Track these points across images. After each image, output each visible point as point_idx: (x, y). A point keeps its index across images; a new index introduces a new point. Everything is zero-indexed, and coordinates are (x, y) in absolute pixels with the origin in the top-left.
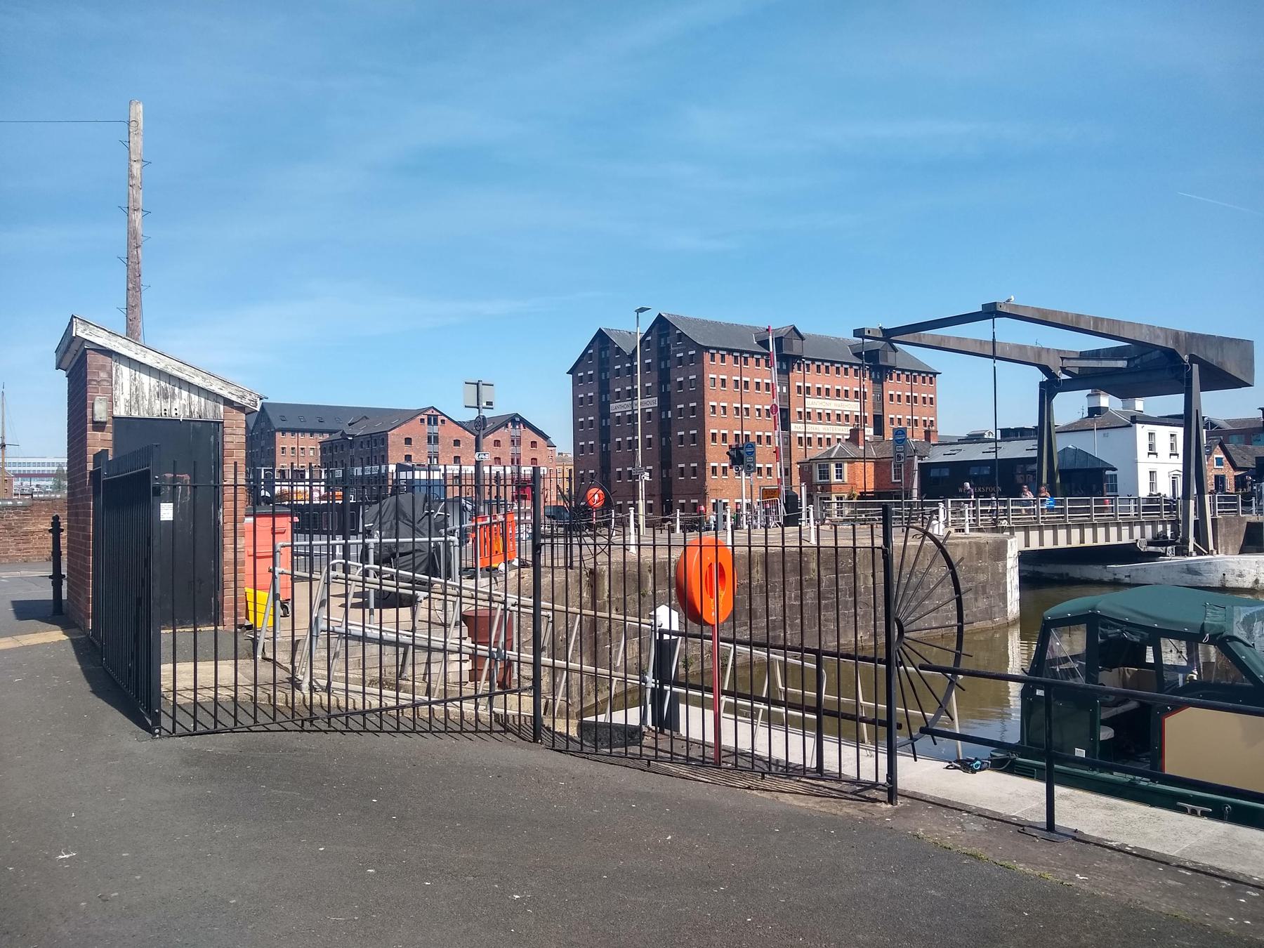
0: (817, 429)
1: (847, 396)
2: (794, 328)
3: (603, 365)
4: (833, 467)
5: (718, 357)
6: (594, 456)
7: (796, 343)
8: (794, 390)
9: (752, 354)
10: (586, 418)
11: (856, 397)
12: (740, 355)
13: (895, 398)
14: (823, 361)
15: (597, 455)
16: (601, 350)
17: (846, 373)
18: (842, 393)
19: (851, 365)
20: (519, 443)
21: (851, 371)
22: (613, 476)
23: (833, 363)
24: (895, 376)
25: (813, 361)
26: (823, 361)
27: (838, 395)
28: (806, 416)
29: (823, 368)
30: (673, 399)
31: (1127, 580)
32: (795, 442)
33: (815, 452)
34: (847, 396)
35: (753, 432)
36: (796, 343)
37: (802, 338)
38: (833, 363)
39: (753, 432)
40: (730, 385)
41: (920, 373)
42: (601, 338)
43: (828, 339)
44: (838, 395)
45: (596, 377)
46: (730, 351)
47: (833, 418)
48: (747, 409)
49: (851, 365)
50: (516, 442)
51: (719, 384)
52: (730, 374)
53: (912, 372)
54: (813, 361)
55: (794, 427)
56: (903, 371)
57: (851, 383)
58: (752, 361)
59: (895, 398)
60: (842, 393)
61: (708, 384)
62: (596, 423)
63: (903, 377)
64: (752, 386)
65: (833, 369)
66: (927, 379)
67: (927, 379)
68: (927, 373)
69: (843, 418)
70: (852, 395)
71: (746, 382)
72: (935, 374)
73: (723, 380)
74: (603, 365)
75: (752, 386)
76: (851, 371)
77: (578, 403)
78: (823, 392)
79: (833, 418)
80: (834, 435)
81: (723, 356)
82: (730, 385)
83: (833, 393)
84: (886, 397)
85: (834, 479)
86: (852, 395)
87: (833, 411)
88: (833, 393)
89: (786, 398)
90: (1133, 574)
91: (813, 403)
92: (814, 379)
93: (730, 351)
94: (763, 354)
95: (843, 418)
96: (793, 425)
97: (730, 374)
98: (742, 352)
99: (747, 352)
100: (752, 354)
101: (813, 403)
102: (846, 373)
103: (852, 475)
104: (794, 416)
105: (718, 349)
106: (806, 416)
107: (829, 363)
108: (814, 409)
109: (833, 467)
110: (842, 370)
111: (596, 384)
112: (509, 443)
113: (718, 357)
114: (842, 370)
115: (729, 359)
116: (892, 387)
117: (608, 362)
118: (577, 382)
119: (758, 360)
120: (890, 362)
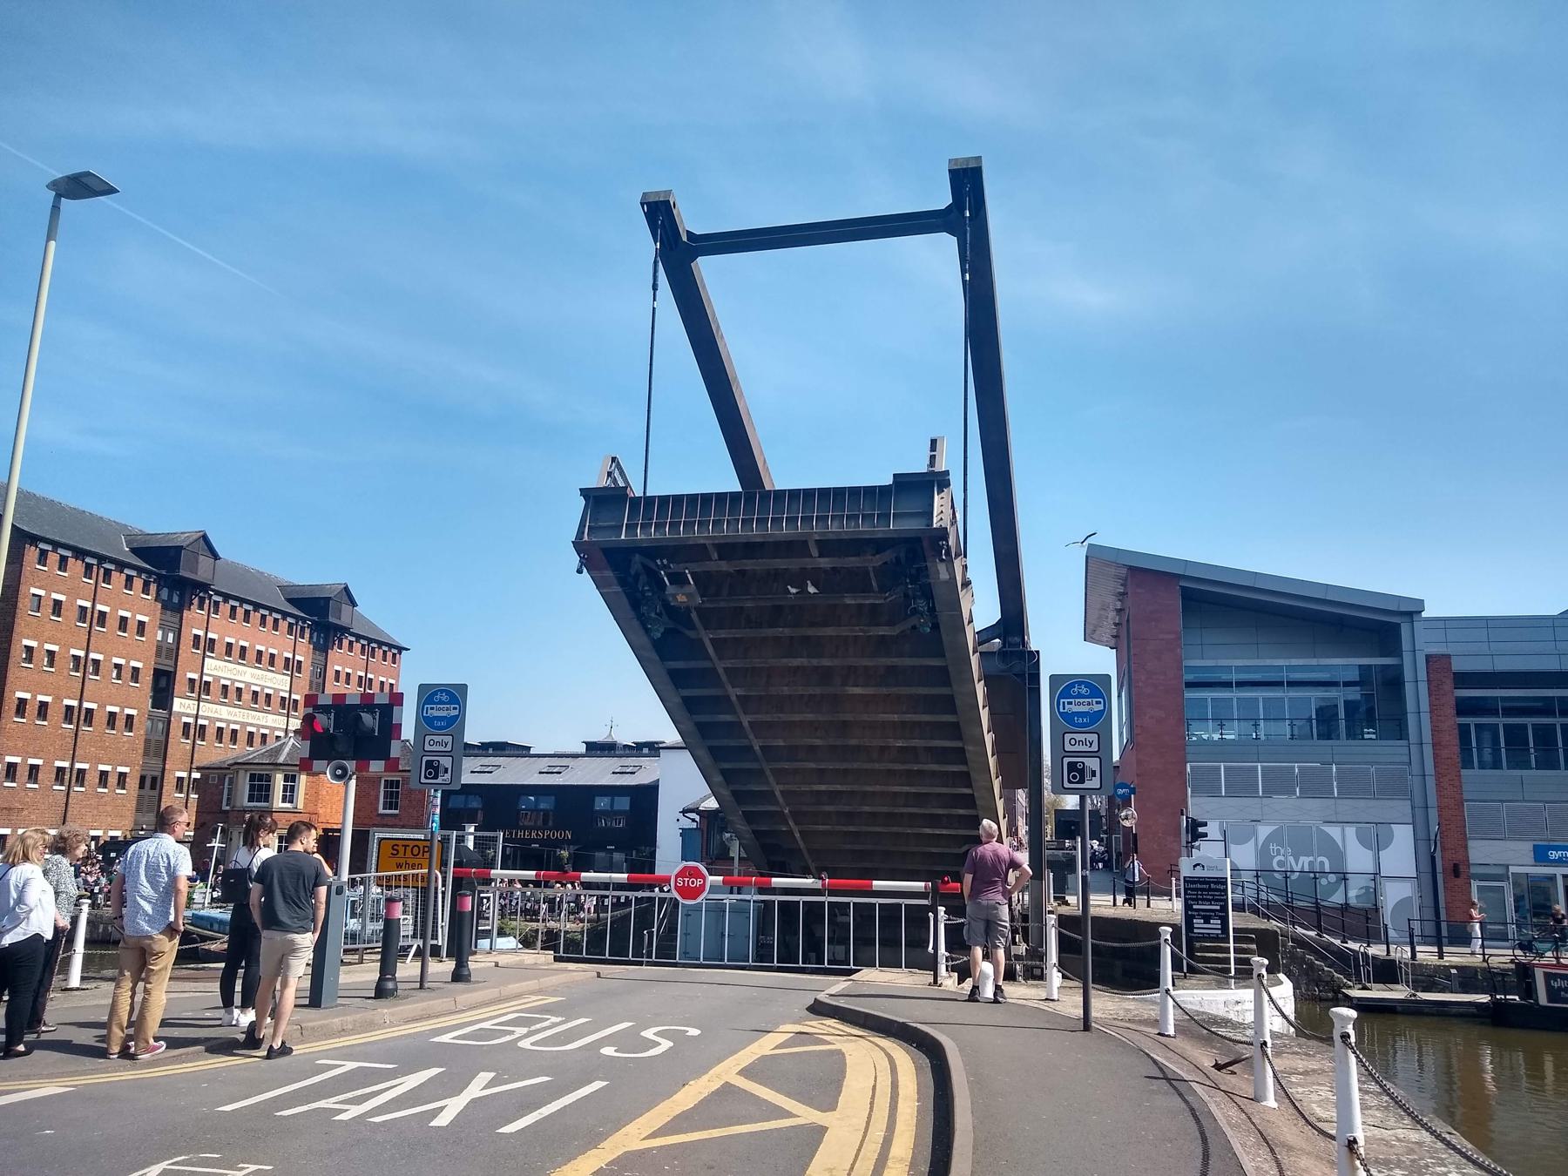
0: (216, 713)
1: (272, 663)
2: (205, 537)
4: (279, 780)
5: (53, 558)
7: (205, 562)
8: (186, 641)
9: (121, 566)
11: (286, 667)
12: (98, 563)
13: (343, 677)
14: (242, 601)
17: (276, 627)
18: (266, 659)
19: (285, 615)
21: (283, 625)
23: (257, 606)
24: (345, 643)
25: (227, 597)
26: (242, 601)
27: (259, 660)
28: (202, 689)
29: (240, 612)
32: (176, 730)
33: (213, 753)
34: (272, 663)
35: (102, 706)
36: (205, 562)
37: (216, 556)
38: (257, 606)
39: (102, 706)
40: (70, 614)
41: (381, 644)
43: (246, 570)
44: (259, 660)
46: (80, 553)
47: (247, 696)
48: (96, 662)
49: (285, 615)
51: (47, 608)
52: (73, 594)
53: (370, 640)
54: (227, 597)
55: (178, 705)
56: (359, 637)
57: (279, 643)
58: (118, 578)
59: (343, 677)
60: (266, 659)
61: (24, 604)
63: (357, 646)
64: (113, 623)
65: (255, 617)
66: (389, 655)
67: (389, 655)
68: (391, 646)
69: (261, 699)
70: (280, 663)
71: (102, 614)
72: (401, 649)
73: (57, 603)
75: (113, 623)
76: (283, 625)
78: (236, 652)
79: (247, 696)
80: (244, 725)
81: (64, 560)
82: (70, 614)
83: (251, 655)
84: (330, 675)
85: (278, 803)
86: (280, 663)
87: (248, 685)
88: (251, 655)
89: (174, 652)
91: (217, 669)
92: (224, 629)
93: (80, 553)
94: (140, 570)
95: (261, 699)
96: (177, 701)
97: (73, 594)
98: (102, 559)
99: (112, 561)
100: (121, 566)
101: (217, 669)
102: (276, 627)
103: (314, 796)
104: (180, 686)
105: (56, 545)
106: (202, 689)
107: (249, 605)
108: (217, 679)
109: (279, 780)
110: (270, 620)
113: (53, 558)
114: (270, 620)
115: (76, 566)
116: (344, 661)
119: (129, 579)
120: (344, 621)
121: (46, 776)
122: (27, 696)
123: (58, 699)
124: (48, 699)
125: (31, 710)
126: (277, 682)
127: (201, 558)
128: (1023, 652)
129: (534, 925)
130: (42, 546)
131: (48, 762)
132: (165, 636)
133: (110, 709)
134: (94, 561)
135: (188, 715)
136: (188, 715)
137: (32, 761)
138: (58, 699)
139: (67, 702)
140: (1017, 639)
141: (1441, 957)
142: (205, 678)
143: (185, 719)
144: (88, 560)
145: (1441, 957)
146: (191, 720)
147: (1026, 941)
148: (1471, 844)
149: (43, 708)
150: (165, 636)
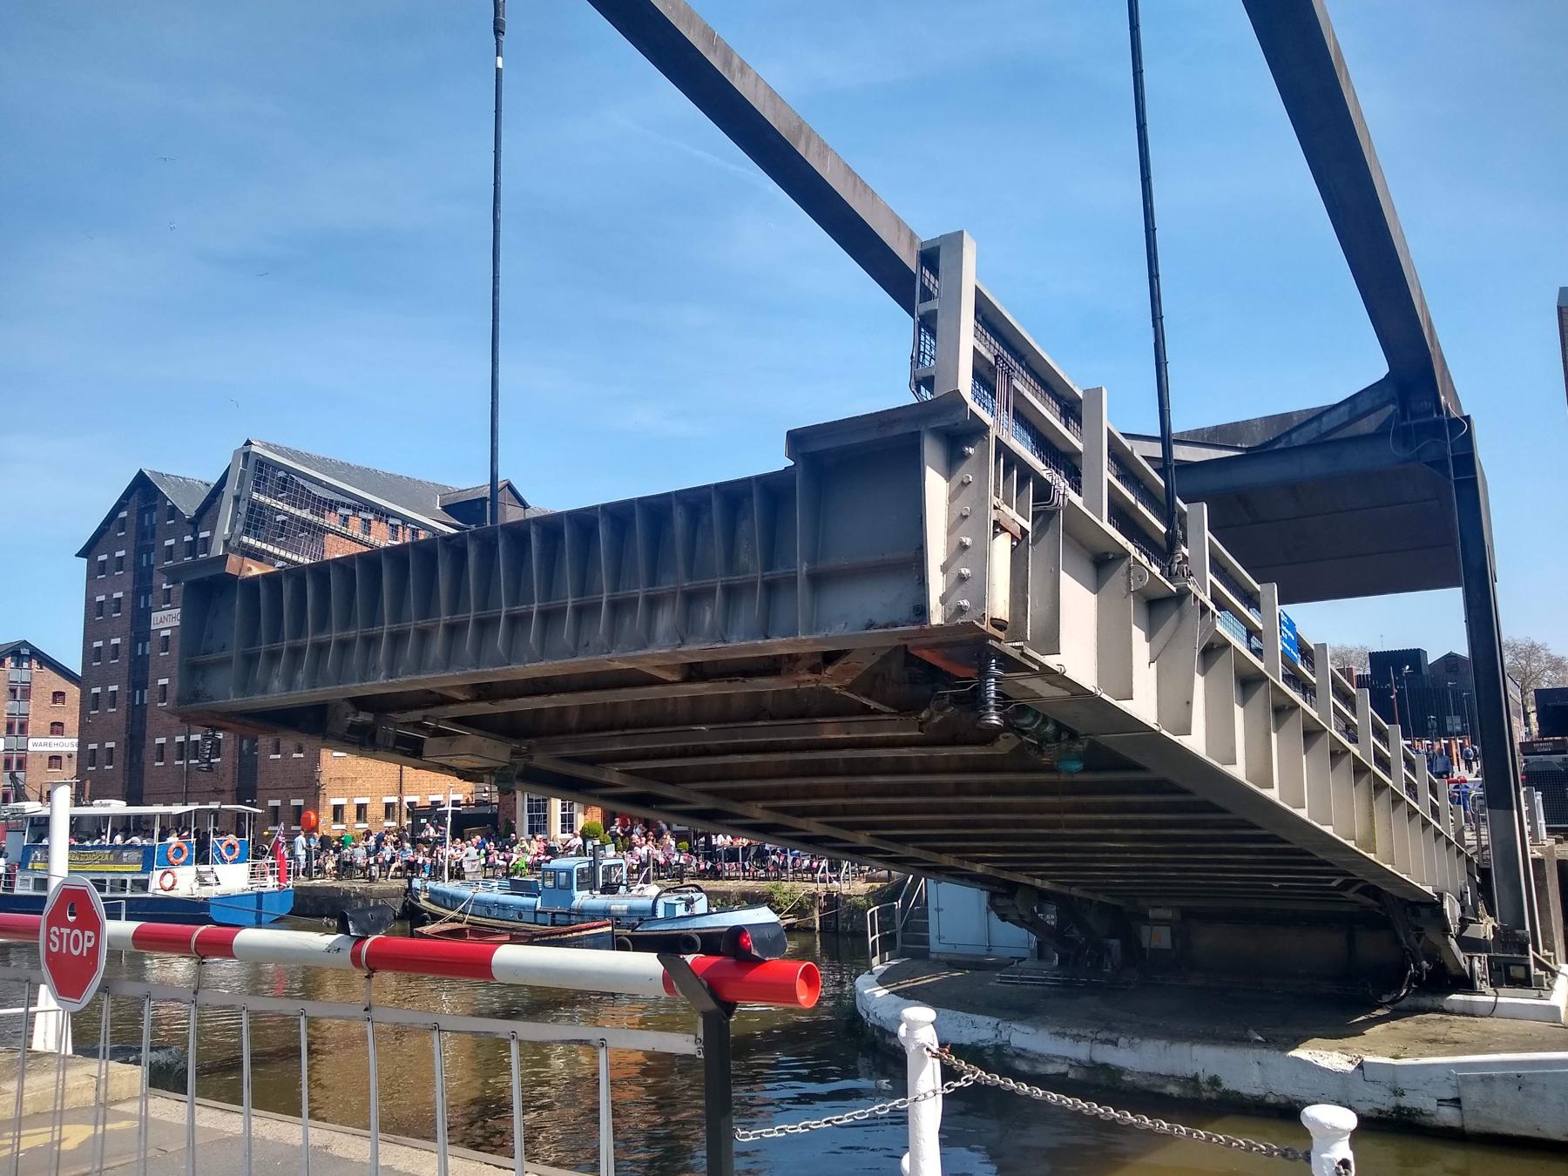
3: (145, 539)
6: (116, 714)
10: (106, 641)
15: (122, 714)
16: (140, 514)
20: (27, 694)
22: (149, 753)
31: (1448, 1116)
42: (143, 489)
45: (128, 563)
50: (19, 692)
62: (124, 652)
74: (145, 539)
77: (95, 613)
90: (1472, 1096)
111: (129, 576)
112: (5, 694)
117: (153, 536)
118: (95, 571)
127: (509, 508)
128: (1439, 425)
129: (812, 887)
130: (341, 511)
134: (399, 522)
140: (1427, 405)
144: (391, 521)
147: (1491, 913)
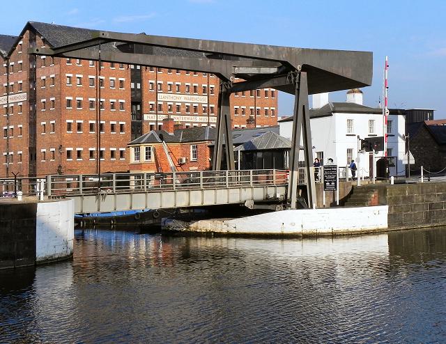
30: (38, 94)
52: (86, 73)
55: (146, 117)
79: (182, 109)
97: (86, 73)
121: (86, 155)
122: (71, 121)
123: (86, 121)
124: (82, 122)
125: (74, 127)
126: (202, 100)
131: (86, 149)
132: (136, 86)
133: (112, 123)
135: (152, 121)
136: (152, 121)
137: (78, 149)
138: (86, 121)
139: (90, 122)
141: (429, 180)
142: (159, 103)
143: (151, 124)
145: (429, 180)
146: (154, 124)
148: (347, 102)
149: (79, 127)
150: (136, 86)
